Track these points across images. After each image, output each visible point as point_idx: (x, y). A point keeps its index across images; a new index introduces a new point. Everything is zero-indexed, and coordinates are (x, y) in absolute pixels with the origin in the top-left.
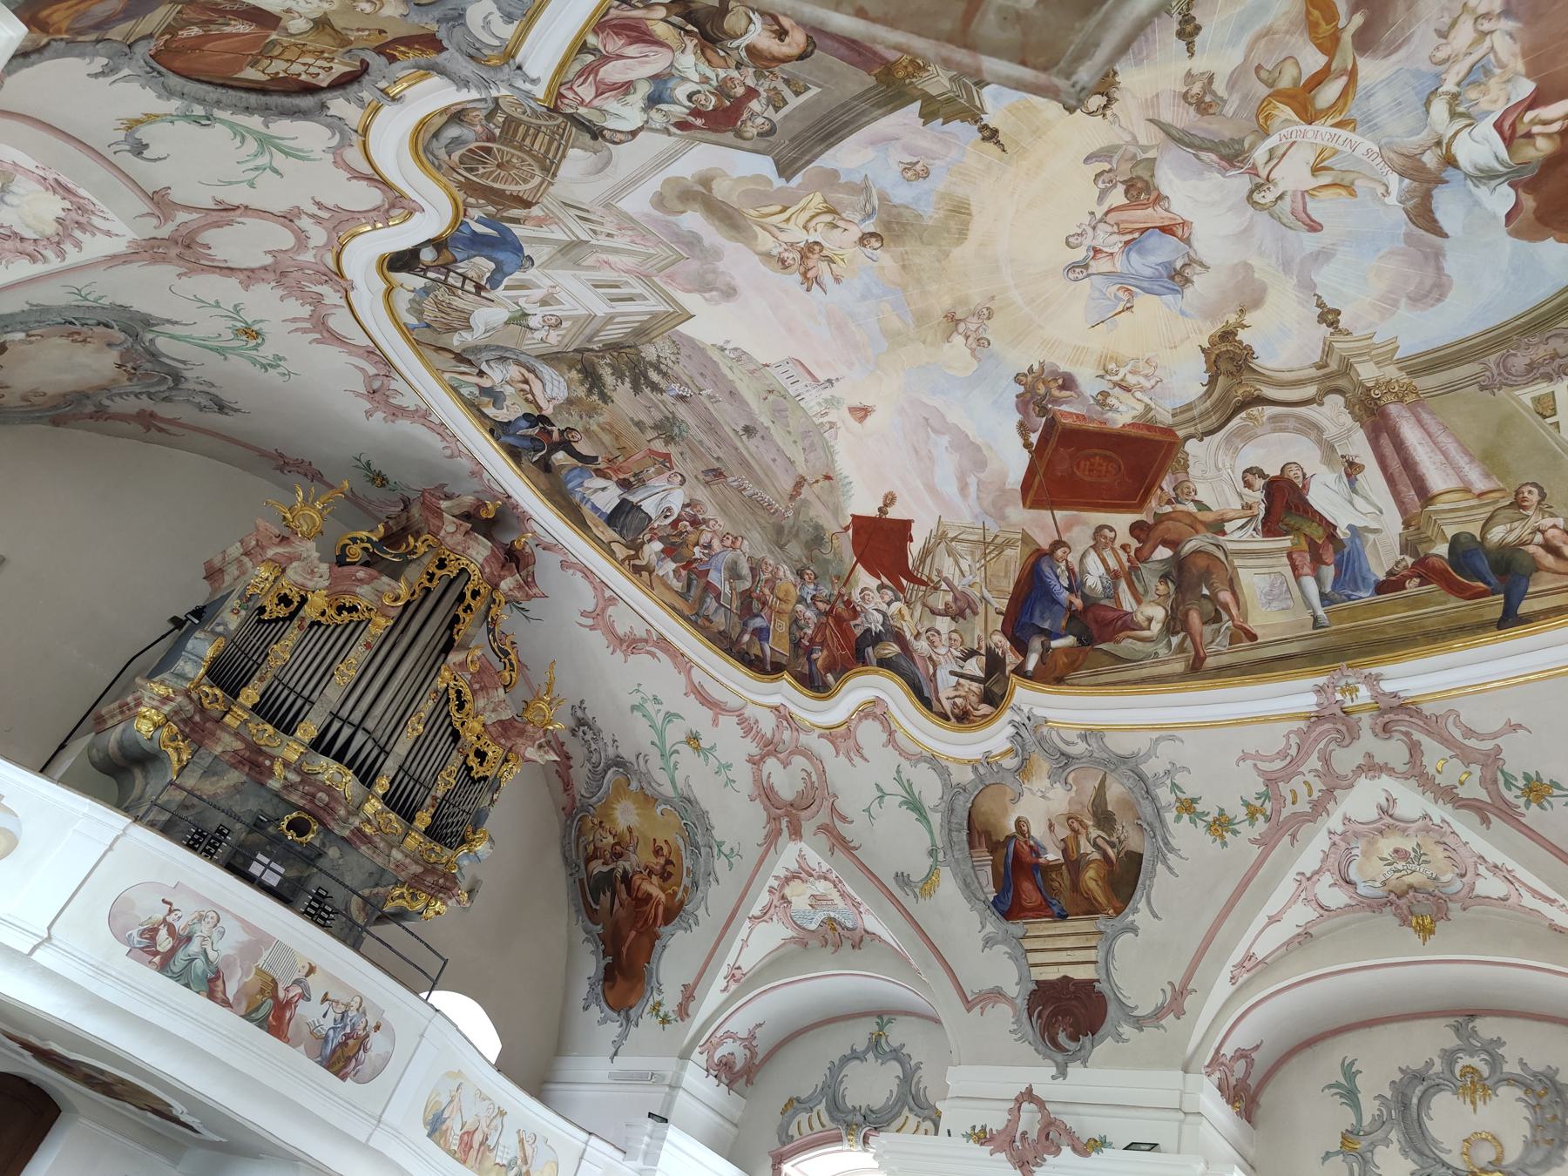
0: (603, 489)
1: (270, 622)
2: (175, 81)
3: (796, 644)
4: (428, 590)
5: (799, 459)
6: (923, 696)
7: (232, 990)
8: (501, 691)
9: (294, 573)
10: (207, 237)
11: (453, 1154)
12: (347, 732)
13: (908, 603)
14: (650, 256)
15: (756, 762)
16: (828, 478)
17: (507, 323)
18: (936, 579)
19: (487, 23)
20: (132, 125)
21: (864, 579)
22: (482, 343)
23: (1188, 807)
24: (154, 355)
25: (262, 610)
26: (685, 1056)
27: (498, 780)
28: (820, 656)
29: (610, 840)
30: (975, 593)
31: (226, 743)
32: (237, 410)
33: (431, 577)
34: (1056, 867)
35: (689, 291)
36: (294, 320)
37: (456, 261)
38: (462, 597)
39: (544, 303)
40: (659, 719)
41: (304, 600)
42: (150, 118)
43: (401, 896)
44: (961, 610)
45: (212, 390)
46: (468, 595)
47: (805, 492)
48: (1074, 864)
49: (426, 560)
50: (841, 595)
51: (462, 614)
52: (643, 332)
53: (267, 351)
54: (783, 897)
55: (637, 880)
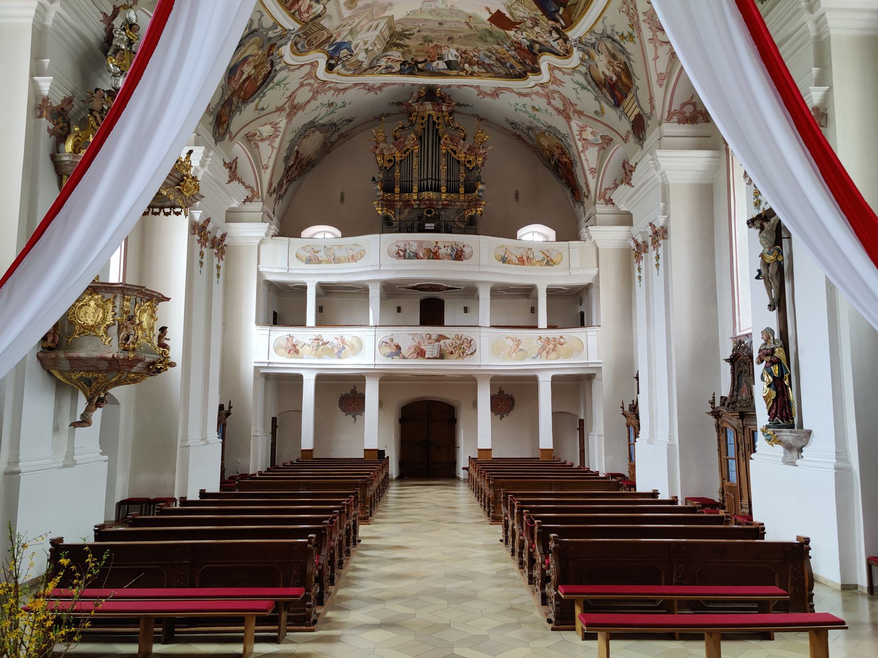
0: (438, 64)
1: (390, 169)
2: (251, 99)
3: (521, 63)
4: (424, 129)
5: (458, 19)
6: (557, 54)
7: (421, 255)
8: (462, 141)
9: (386, 153)
10: (296, 102)
11: (518, 264)
12: (425, 182)
13: (525, 31)
14: (366, 16)
15: (549, 104)
16: (470, 17)
17: (367, 54)
18: (521, 19)
19: (275, 33)
20: (256, 109)
21: (511, 33)
22: (369, 61)
23: (622, 36)
24: (323, 125)
25: (386, 168)
26: (595, 204)
27: (477, 165)
28: (528, 61)
29: (548, 152)
30: (532, 15)
31: (399, 204)
32: (354, 118)
33: (422, 124)
34: (617, 81)
35: (384, 13)
36: (333, 95)
37: (338, 57)
38: (434, 123)
39: (366, 43)
40: (523, 108)
41: (394, 157)
42: (258, 104)
43: (468, 213)
44: (536, 23)
45: (343, 119)
46: (436, 121)
47: (472, 25)
48: (619, 76)
49: (418, 121)
50: (512, 42)
51: (438, 127)
52: (390, 28)
53: (339, 104)
54: (584, 139)
55: (561, 160)
